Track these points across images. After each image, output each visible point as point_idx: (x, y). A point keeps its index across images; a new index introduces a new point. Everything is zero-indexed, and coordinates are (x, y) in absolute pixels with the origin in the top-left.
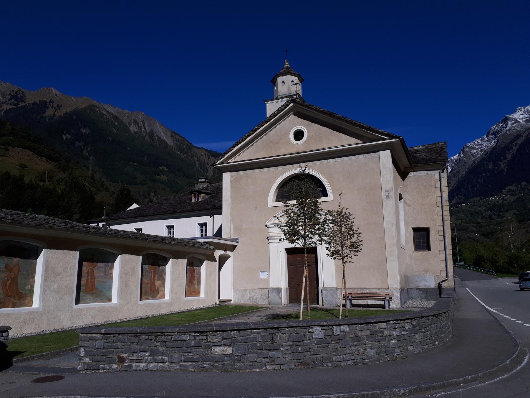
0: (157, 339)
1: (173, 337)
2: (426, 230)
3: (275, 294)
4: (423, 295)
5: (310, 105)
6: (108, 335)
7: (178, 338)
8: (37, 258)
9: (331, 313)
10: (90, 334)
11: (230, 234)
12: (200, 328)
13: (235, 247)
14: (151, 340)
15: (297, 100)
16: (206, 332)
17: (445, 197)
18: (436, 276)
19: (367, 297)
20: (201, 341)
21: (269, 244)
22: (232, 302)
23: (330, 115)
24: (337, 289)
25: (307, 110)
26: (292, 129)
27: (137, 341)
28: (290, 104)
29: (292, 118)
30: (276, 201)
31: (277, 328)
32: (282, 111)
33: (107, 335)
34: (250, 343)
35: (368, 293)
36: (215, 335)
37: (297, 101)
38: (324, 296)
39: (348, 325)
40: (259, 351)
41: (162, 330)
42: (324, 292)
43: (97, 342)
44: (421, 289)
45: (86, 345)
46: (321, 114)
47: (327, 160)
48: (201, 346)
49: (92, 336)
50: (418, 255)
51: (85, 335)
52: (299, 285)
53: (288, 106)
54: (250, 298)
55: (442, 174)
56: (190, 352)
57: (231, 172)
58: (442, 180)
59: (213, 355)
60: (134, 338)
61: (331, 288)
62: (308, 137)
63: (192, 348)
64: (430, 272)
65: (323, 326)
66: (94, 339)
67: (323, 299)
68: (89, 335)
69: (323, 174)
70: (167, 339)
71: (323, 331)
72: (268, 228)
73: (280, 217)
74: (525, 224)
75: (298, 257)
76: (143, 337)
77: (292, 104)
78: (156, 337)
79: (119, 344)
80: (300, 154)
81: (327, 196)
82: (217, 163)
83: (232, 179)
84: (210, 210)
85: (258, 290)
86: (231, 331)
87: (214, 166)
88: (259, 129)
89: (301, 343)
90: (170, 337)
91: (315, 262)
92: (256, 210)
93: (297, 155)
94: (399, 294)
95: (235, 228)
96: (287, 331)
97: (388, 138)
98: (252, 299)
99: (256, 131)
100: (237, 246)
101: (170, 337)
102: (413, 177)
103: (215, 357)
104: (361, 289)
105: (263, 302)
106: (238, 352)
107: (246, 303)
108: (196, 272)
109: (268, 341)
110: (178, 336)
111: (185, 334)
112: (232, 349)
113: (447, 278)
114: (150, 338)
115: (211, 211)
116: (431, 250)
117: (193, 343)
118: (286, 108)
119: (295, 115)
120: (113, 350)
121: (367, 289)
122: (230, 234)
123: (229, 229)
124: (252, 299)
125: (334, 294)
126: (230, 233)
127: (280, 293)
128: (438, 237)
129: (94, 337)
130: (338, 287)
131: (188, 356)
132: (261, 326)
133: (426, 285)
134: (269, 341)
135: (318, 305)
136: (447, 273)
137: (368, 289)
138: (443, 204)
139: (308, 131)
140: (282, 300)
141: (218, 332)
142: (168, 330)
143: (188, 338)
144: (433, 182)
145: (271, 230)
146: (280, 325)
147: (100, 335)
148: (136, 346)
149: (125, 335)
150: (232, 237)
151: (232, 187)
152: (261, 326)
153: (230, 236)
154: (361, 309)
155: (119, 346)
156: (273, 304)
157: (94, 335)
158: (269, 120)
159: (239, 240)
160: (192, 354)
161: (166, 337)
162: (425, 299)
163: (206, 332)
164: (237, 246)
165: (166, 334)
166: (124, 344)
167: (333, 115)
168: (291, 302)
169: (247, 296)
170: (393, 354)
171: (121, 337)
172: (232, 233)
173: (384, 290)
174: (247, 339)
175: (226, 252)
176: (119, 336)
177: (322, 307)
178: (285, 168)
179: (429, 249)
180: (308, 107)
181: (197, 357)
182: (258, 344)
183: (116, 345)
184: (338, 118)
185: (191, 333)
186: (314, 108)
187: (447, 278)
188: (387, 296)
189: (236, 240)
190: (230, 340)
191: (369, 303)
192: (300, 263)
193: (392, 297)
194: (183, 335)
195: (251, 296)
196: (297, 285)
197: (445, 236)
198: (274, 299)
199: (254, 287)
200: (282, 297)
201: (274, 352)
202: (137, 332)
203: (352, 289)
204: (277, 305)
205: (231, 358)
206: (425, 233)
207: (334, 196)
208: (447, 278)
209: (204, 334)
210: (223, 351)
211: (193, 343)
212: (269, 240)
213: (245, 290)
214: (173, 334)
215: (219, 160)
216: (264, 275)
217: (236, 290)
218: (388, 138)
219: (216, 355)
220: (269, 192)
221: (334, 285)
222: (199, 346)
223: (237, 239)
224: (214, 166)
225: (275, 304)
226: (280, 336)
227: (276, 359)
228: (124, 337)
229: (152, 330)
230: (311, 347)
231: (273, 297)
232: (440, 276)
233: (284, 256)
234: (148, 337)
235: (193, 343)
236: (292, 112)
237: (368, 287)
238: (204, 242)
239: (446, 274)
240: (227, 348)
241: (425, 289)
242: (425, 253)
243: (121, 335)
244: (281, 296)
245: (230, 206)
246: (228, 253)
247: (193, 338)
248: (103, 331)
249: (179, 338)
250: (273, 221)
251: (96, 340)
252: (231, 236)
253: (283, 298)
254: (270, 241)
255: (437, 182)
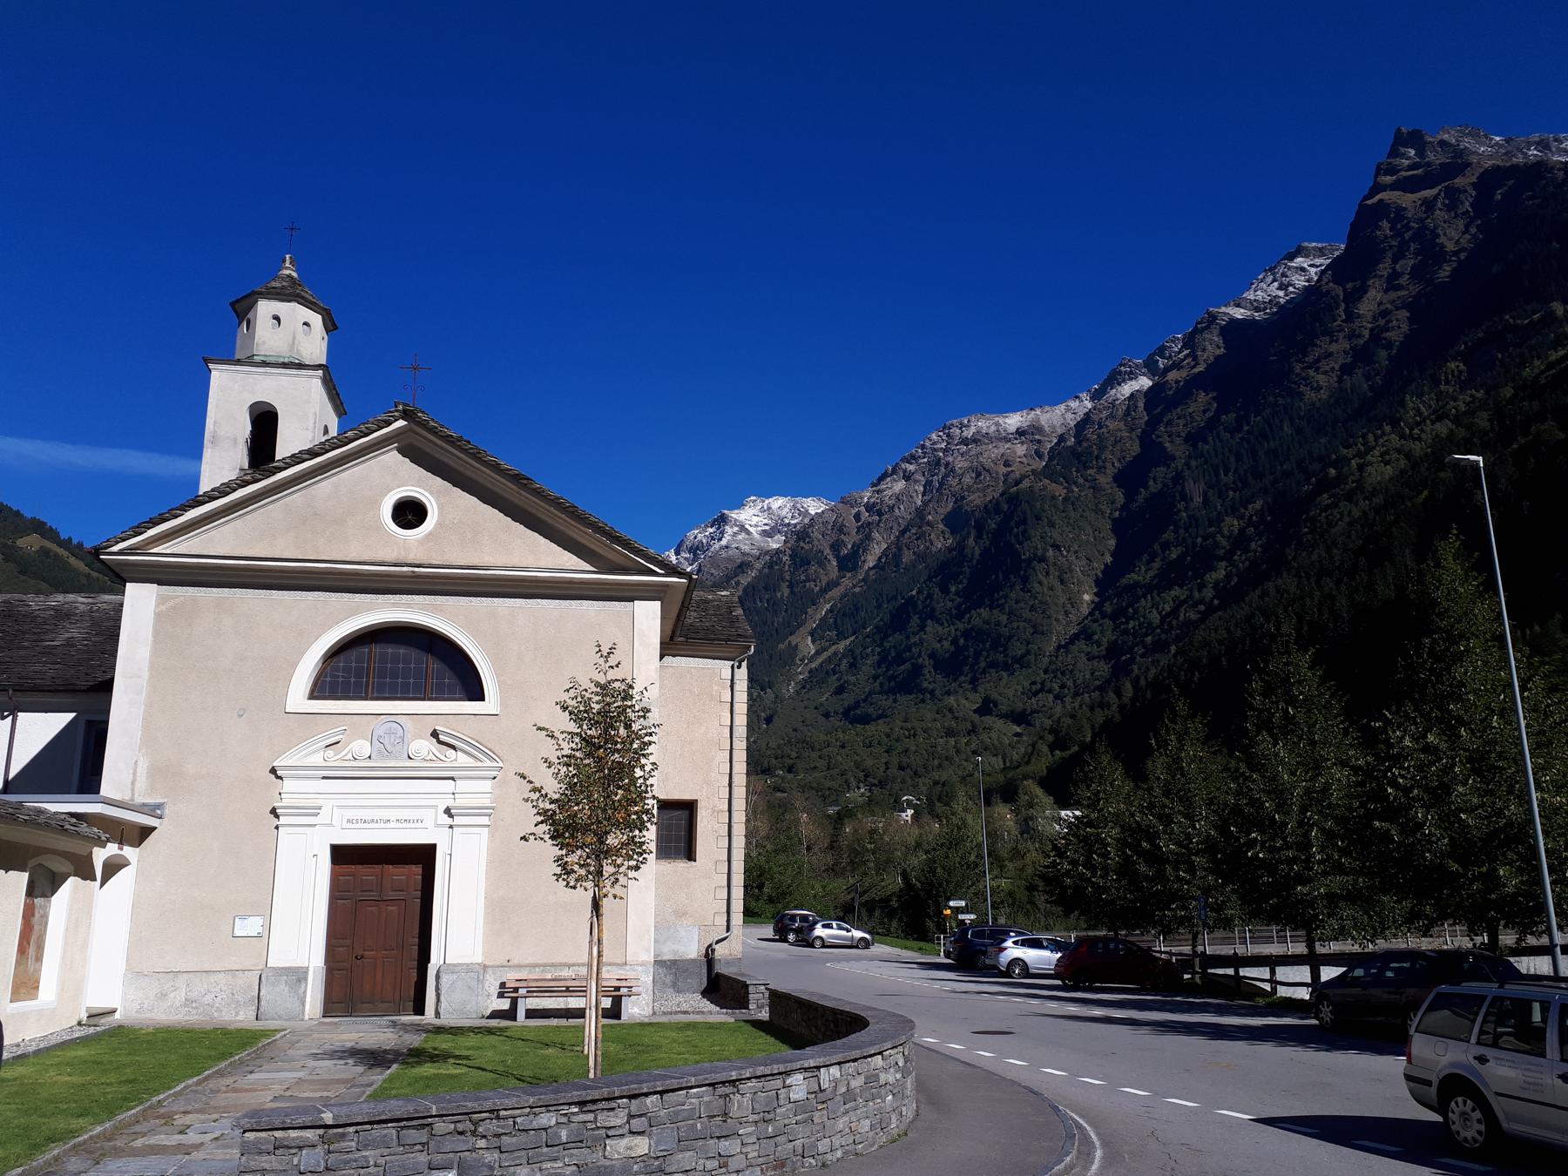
0: (480, 1129)
1: (519, 1120)
2: (689, 807)
3: (283, 987)
4: (669, 979)
5: (460, 439)
6: (340, 1130)
7: (532, 1121)
8: (54, 892)
9: (507, 1037)
10: (280, 1132)
11: (133, 790)
12: (584, 1093)
13: (146, 832)
14: (461, 1133)
15: (420, 415)
16: (594, 1102)
17: (740, 728)
18: (704, 928)
19: (568, 988)
20: (581, 1126)
21: (277, 828)
22: (117, 1016)
23: (517, 478)
24: (485, 967)
25: (442, 448)
26: (389, 492)
27: (425, 1141)
28: (396, 420)
29: (391, 458)
30: (312, 696)
31: (733, 1082)
32: (366, 435)
33: (335, 1131)
34: (683, 1123)
35: (573, 977)
36: (613, 1109)
37: (419, 417)
38: (443, 992)
39: (839, 1063)
40: (701, 1143)
41: (495, 1104)
42: (444, 979)
43: (304, 1152)
44: (665, 961)
45: (267, 1166)
46: (488, 471)
47: (490, 599)
48: (581, 1142)
49: (286, 1135)
50: (665, 873)
51: (263, 1134)
52: (362, 957)
53: (390, 424)
54: (189, 1002)
55: (736, 670)
56: (555, 1160)
57: (160, 583)
58: (737, 687)
59: (607, 1163)
60: (415, 1131)
61: (467, 965)
62: (439, 525)
63: (561, 1147)
64: (690, 916)
65: (806, 1069)
66: (293, 1145)
67: (442, 998)
68: (278, 1134)
69: (475, 634)
70: (503, 1127)
71: (806, 1082)
72: (281, 778)
73: (327, 747)
74: (937, 817)
75: (368, 873)
76: (441, 1126)
77: (401, 423)
78: (476, 1124)
79: (372, 1152)
80: (416, 569)
81: (483, 699)
82: (115, 549)
83: (163, 608)
84: (11, 692)
85: (221, 975)
86: (646, 1095)
87: (101, 557)
88: (286, 469)
89: (771, 1116)
90: (511, 1121)
91: (420, 888)
92: (242, 719)
93: (405, 569)
94: (651, 978)
95: (156, 772)
96: (750, 1088)
97: (663, 572)
98: (194, 1005)
99: (274, 474)
100: (156, 828)
101: (511, 1121)
102: (670, 669)
103: (613, 1166)
104: (553, 965)
105: (237, 1014)
106: (661, 1149)
107: (171, 1018)
108: (37, 915)
109: (715, 1116)
110: (532, 1116)
111: (549, 1111)
112: (648, 1141)
113: (727, 932)
114: (460, 1127)
115: (10, 699)
116: (697, 859)
117: (564, 1135)
118: (382, 428)
119: (403, 452)
120: (352, 1171)
121: (569, 966)
122: (133, 790)
123: (132, 771)
124: (194, 1005)
125: (474, 984)
126: (133, 783)
127: (303, 985)
128: (717, 826)
129: (294, 1139)
130: (487, 963)
131: (551, 1171)
132: (706, 1079)
133: (675, 952)
134: (719, 1116)
135: (423, 1017)
136: (728, 921)
137: (574, 965)
138: (734, 743)
139: (441, 508)
140: (304, 1006)
141: (620, 1101)
142: (508, 1102)
143: (553, 1122)
144: (716, 688)
145: (288, 785)
146: (741, 1075)
147: (312, 1130)
148: (419, 1154)
149: (389, 1125)
150: (139, 800)
151: (157, 633)
152: (706, 1079)
153: (133, 794)
154: (554, 1022)
155: (370, 1159)
156: (274, 1019)
157: (293, 1134)
158: (323, 451)
159: (167, 811)
160: (561, 1165)
161: (502, 1123)
162: (672, 990)
163: (594, 1102)
164: (156, 828)
165: (502, 1113)
166: (386, 1152)
167: (525, 482)
168: (327, 1012)
169: (178, 997)
170: (889, 1128)
171: (378, 1132)
172: (142, 783)
173: (614, 967)
174: (676, 1113)
175: (122, 849)
176: (372, 1129)
177: (438, 1022)
178: (356, 600)
179: (690, 855)
180: (453, 442)
181: (573, 1171)
182: (699, 1125)
183: (363, 1157)
184: (538, 493)
185: (562, 1107)
186: (471, 451)
187: (727, 932)
188: (623, 983)
189: (153, 810)
190: (643, 1118)
191: (570, 1006)
192: (372, 891)
193: (631, 987)
194: (542, 1115)
195: (194, 995)
196: (356, 957)
197: (733, 824)
198: (279, 1002)
199: (207, 967)
200: (305, 997)
201: (726, 1141)
202: (429, 1114)
203: (526, 966)
204: (286, 1020)
205: (646, 1166)
206: (684, 814)
207: (504, 704)
208: (728, 934)
209: (590, 1107)
210: (630, 1148)
211: (565, 1133)
212: (277, 816)
213: (171, 975)
214: (518, 1112)
215: (123, 540)
216: (251, 926)
217: (134, 973)
218: (663, 572)
219: (614, 1162)
220: (294, 665)
221: (478, 958)
222: (577, 1142)
223: (159, 806)
224: (101, 557)
225: (280, 1018)
226: (738, 1101)
227: (730, 1159)
228: (386, 1131)
229: (469, 1104)
230: (786, 1122)
231: (276, 997)
232: (714, 928)
233: (322, 870)
234: (455, 1127)
235: (564, 1135)
236: (396, 445)
237: (571, 961)
238: (72, 815)
239: (726, 924)
240: (638, 1140)
241: (674, 962)
242: (681, 865)
243: (379, 1126)
244: (305, 992)
245: (144, 695)
246: (128, 851)
247: (564, 1120)
248: (328, 1118)
249: (534, 1123)
250: (300, 759)
251: (300, 1148)
252: (136, 796)
253: (308, 1000)
254: (283, 820)
255: (724, 688)
